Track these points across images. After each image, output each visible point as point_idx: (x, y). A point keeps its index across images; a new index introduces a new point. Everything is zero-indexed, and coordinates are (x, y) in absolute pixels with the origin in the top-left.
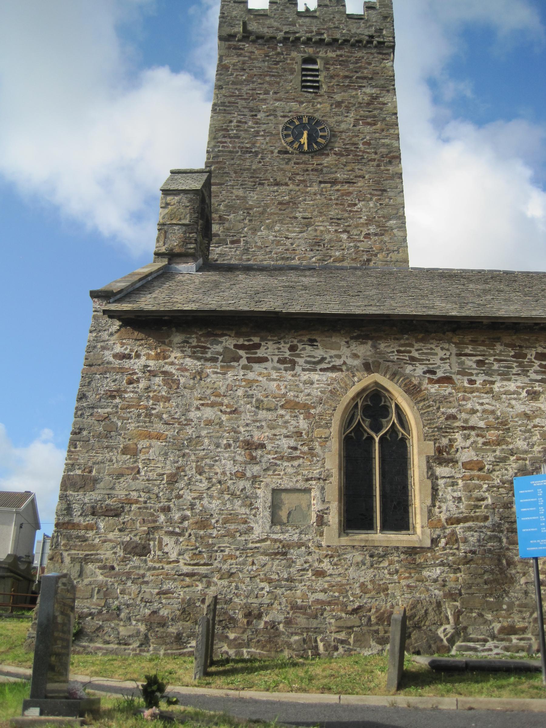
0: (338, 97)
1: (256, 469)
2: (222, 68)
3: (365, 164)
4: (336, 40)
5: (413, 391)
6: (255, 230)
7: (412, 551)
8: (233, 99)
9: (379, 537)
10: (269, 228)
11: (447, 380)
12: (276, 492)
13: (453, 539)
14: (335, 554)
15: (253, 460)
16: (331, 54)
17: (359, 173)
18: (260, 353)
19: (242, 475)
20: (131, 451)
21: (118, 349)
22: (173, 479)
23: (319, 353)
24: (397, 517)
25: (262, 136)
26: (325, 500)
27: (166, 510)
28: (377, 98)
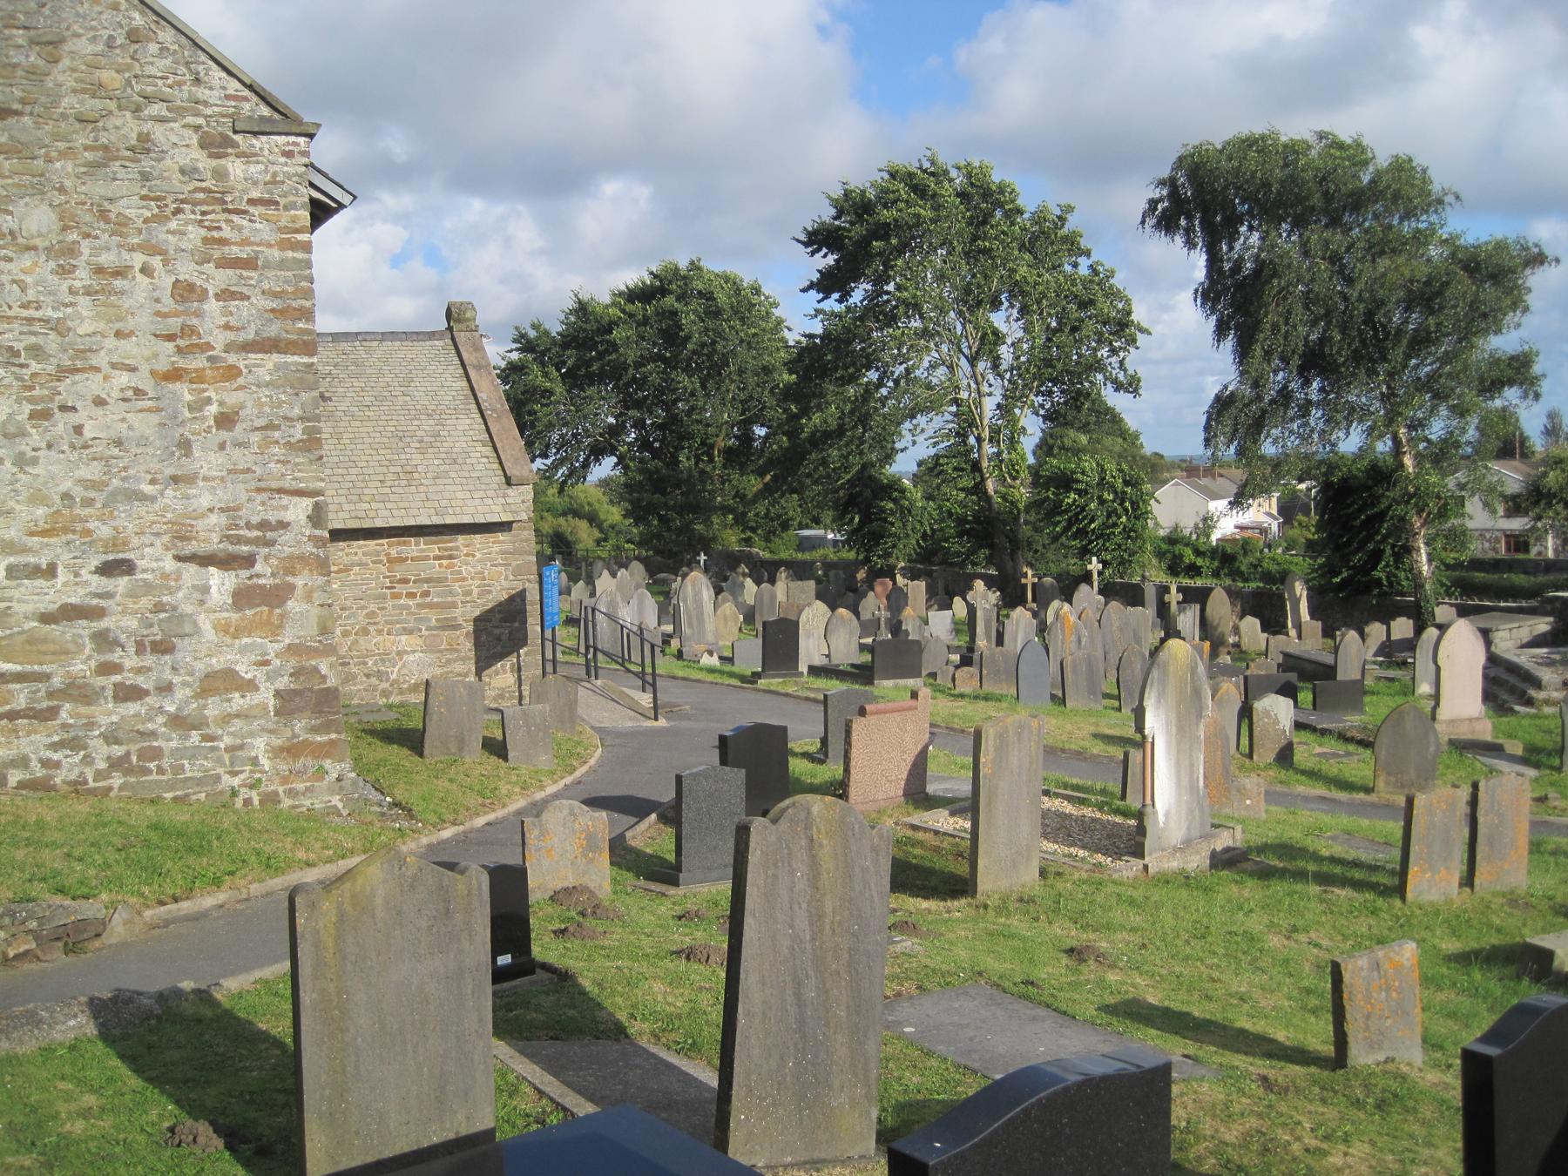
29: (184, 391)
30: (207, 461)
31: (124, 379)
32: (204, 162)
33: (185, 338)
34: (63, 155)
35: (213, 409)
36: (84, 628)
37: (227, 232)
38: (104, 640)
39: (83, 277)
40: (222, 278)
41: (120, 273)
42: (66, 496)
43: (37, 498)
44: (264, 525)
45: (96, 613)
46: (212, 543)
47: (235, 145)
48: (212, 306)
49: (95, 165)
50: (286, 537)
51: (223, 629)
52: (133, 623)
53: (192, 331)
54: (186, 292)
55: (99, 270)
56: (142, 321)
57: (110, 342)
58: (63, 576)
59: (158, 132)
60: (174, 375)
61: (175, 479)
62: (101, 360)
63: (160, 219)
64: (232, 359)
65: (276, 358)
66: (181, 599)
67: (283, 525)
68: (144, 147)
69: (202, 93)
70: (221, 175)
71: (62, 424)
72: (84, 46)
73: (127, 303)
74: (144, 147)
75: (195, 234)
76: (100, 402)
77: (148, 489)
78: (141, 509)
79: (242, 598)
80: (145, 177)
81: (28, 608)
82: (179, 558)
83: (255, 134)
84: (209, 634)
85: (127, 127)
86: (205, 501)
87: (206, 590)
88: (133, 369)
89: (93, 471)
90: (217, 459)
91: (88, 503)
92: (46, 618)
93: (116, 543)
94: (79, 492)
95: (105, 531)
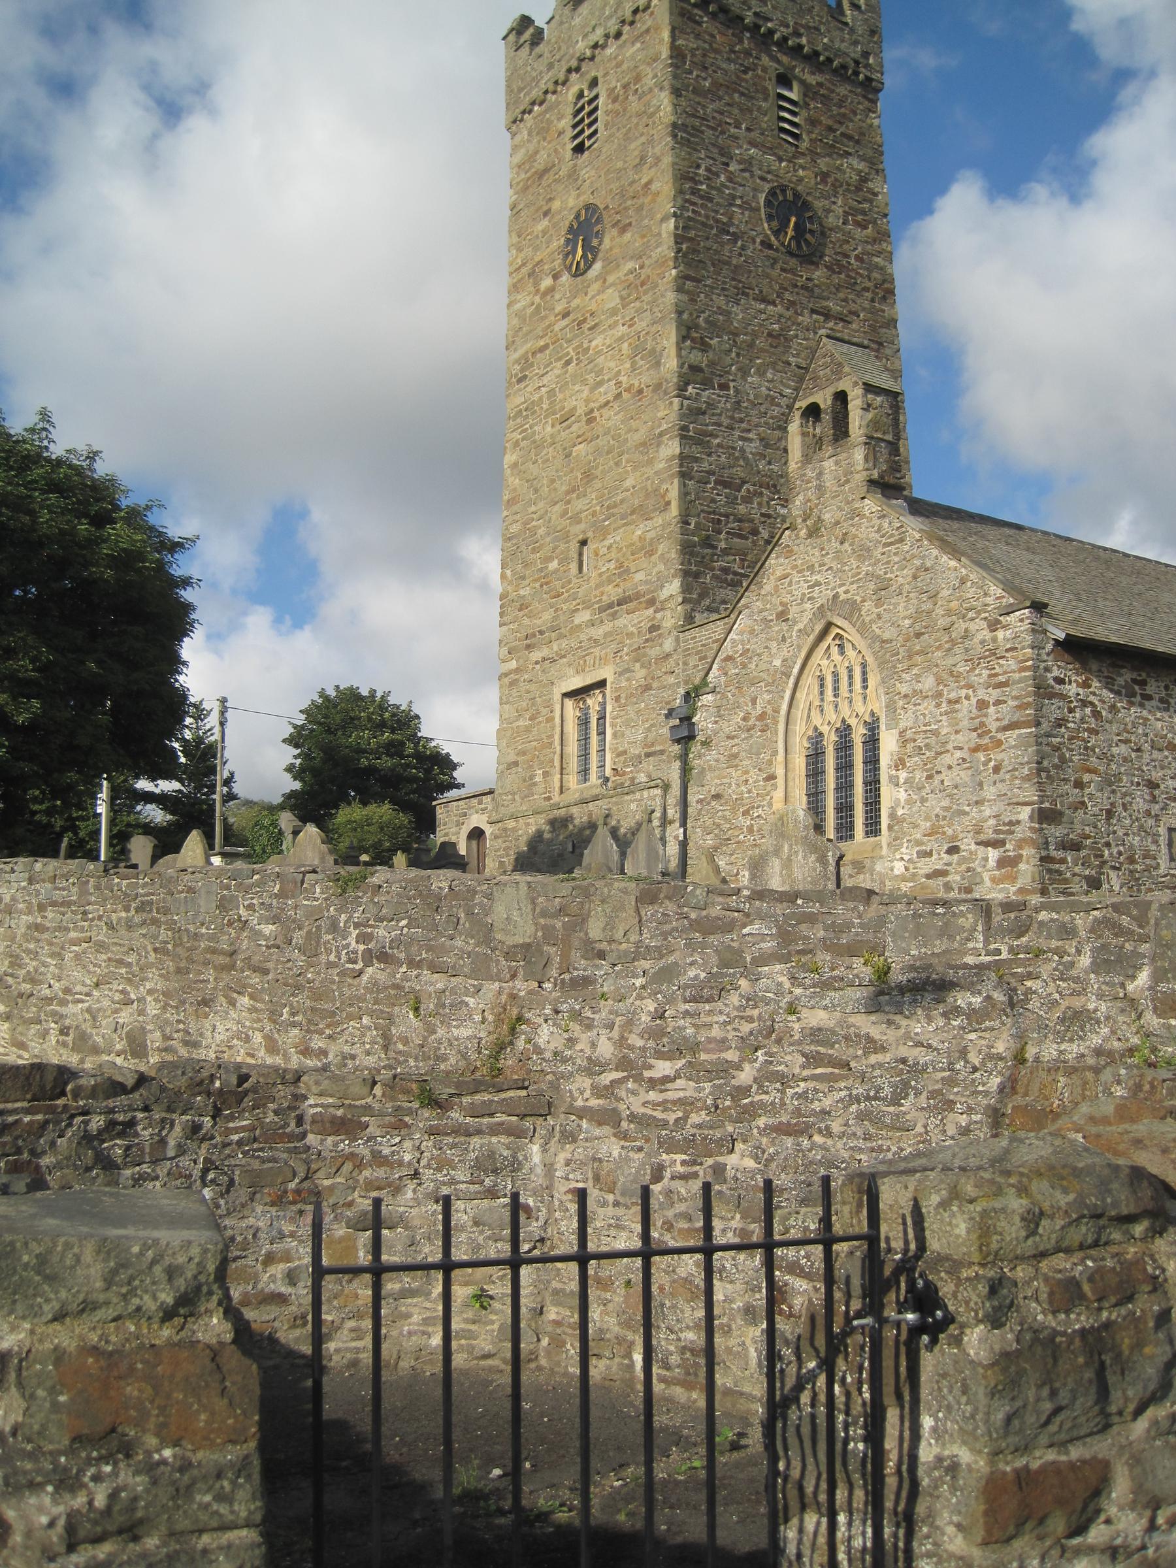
0: (823, 163)
1: (1156, 809)
2: (677, 54)
3: (859, 295)
4: (817, 54)
6: (745, 372)
10: (761, 373)
16: (812, 79)
18: (1149, 690)
20: (1079, 784)
22: (1110, 814)
25: (739, 206)
27: (1108, 845)
29: (981, 756)
30: (990, 792)
31: (958, 754)
32: (986, 634)
33: (980, 729)
34: (938, 648)
35: (992, 764)
36: (941, 881)
37: (998, 670)
39: (944, 707)
40: (995, 694)
41: (957, 701)
42: (937, 816)
43: (927, 819)
44: (1011, 823)
45: (941, 873)
46: (989, 835)
47: (999, 622)
48: (992, 709)
49: (949, 650)
50: (1018, 829)
51: (993, 880)
52: (958, 878)
53: (982, 724)
54: (982, 705)
55: (950, 702)
56: (965, 723)
57: (953, 737)
58: (935, 856)
59: (973, 627)
60: (976, 749)
61: (977, 803)
62: (950, 747)
63: (972, 670)
64: (999, 736)
65: (1017, 732)
66: (975, 865)
67: (1018, 822)
68: (967, 635)
69: (989, 600)
70: (995, 640)
71: (937, 778)
72: (945, 593)
73: (960, 715)
74: (967, 635)
75: (985, 673)
76: (950, 767)
77: (967, 809)
78: (965, 819)
79: (1002, 863)
80: (967, 650)
81: (922, 872)
82: (977, 844)
83: (1008, 614)
84: (988, 883)
85: (961, 625)
86: (988, 813)
87: (986, 859)
88: (961, 749)
89: (945, 803)
90: (993, 789)
91: (944, 818)
92: (928, 877)
93: (954, 838)
94: (941, 813)
95: (950, 832)
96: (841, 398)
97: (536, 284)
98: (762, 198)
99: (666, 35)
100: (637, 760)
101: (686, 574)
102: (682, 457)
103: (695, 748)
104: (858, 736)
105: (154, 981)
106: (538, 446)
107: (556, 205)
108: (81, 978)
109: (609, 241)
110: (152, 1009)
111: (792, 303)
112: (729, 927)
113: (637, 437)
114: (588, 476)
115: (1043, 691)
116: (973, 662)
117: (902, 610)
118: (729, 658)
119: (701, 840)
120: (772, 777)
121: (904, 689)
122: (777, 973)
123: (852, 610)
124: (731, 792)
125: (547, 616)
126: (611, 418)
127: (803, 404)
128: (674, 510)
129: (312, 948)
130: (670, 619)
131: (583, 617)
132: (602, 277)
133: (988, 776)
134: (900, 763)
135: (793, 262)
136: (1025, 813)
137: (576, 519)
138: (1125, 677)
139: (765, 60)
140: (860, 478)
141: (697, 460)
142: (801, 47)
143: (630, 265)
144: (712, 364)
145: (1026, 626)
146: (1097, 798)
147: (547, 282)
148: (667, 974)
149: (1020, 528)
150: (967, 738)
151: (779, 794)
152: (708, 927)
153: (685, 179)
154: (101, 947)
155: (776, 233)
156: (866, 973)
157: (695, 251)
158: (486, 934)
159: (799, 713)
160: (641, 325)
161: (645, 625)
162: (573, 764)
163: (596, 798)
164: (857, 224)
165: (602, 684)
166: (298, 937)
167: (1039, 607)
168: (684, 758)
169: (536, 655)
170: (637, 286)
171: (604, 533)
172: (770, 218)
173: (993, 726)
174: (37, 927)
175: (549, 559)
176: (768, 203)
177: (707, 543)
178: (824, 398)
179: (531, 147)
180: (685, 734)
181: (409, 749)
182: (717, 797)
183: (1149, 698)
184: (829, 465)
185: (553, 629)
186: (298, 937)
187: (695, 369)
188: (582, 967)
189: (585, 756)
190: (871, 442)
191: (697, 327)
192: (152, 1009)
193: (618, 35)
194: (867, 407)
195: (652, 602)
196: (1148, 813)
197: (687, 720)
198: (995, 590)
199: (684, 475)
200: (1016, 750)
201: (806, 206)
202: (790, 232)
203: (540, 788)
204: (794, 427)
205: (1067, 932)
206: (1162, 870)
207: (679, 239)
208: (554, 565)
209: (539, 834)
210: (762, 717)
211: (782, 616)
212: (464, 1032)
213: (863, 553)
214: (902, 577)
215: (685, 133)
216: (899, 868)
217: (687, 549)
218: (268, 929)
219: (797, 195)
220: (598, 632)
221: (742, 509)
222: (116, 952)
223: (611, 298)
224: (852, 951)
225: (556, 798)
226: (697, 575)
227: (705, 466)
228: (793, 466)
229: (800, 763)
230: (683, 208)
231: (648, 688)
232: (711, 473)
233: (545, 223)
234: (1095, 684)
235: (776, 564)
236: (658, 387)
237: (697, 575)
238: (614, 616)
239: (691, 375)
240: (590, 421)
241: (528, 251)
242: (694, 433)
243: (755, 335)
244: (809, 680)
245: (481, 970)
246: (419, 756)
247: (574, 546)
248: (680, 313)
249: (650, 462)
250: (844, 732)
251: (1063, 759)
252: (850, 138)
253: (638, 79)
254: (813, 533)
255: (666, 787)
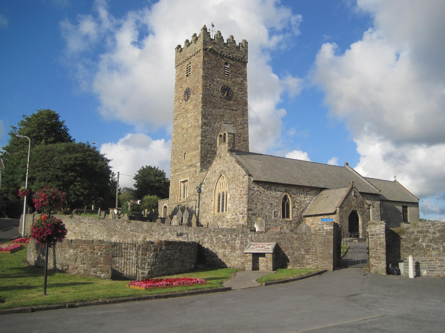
0: (233, 80)
2: (204, 62)
3: (240, 105)
4: (233, 58)
5: (291, 196)
6: (215, 123)
7: (290, 221)
8: (207, 75)
9: (286, 219)
10: (218, 123)
11: (294, 194)
12: (275, 212)
13: (295, 220)
14: (282, 222)
15: (272, 207)
16: (232, 63)
17: (238, 108)
19: (270, 209)
20: (256, 204)
21: (252, 186)
22: (262, 209)
23: (279, 188)
24: (288, 217)
26: (280, 214)
28: (242, 82)
30: (241, 205)
33: (241, 195)
38: (235, 221)
46: (241, 212)
54: (241, 191)
56: (239, 194)
60: (240, 198)
96: (225, 134)
97: (179, 101)
98: (220, 88)
99: (202, 58)
100: (192, 195)
101: (201, 162)
102: (201, 140)
103: (201, 194)
104: (225, 193)
105: (105, 233)
106: (178, 133)
107: (183, 86)
108: (96, 233)
109: (191, 96)
110: (105, 237)
111: (225, 108)
112: (165, 229)
113: (194, 135)
114: (186, 141)
115: (249, 189)
116: (240, 184)
117: (231, 173)
118: (207, 178)
119: (201, 210)
120: (212, 200)
121: (231, 187)
122: (169, 233)
123: (224, 172)
124: (206, 203)
125: (179, 166)
126: (190, 130)
127: (219, 134)
128: (200, 150)
129: (124, 230)
130: (198, 170)
131: (185, 168)
132: (190, 103)
133: (241, 203)
134: (230, 200)
135: (226, 100)
136: (246, 209)
137: (184, 149)
138: (267, 186)
139: (222, 60)
140: (227, 149)
141: (204, 140)
142: (230, 57)
143: (195, 102)
144: (208, 122)
145: (247, 178)
146: (259, 206)
147: (181, 101)
148: (159, 233)
149: (261, 155)
150: (239, 196)
151: (213, 203)
152: (163, 229)
153: (204, 86)
154: (98, 229)
155: (223, 95)
156: (176, 234)
157: (206, 100)
158: (143, 229)
159: (217, 189)
160: (196, 114)
161: (194, 171)
162: (182, 195)
163: (185, 202)
164: (240, 91)
165: (187, 180)
166: (123, 228)
167: (250, 175)
168: (199, 196)
169: (176, 174)
170: (195, 106)
171: (188, 152)
172: (221, 92)
173: (242, 194)
174: (90, 226)
175: (179, 156)
176: (221, 89)
177: (206, 156)
178: (222, 134)
179: (179, 73)
180: (200, 191)
181: (163, 181)
182: (204, 203)
183: (272, 189)
184: (223, 146)
185: (179, 169)
186: (123, 228)
187: (205, 123)
188: (152, 232)
189: (184, 194)
190: (229, 143)
191: (205, 115)
192: (105, 237)
193: (194, 55)
194: (229, 137)
195: (195, 166)
196: (270, 209)
197: (200, 189)
198: (244, 172)
199: (202, 143)
200: (245, 199)
201: (229, 89)
202: (226, 95)
203: (176, 199)
204: (218, 138)
205: (191, 230)
206: (273, 218)
207: (203, 98)
208: (180, 157)
209: (176, 208)
210: (211, 189)
211: (215, 172)
212: (140, 239)
213: (227, 163)
214: (232, 168)
215: (205, 77)
216: (229, 217)
217: (202, 157)
218: (120, 227)
219: (227, 87)
220: (187, 171)
221: (213, 149)
222: (100, 229)
223: (191, 107)
224: (175, 231)
225: (179, 201)
226: (203, 162)
227: (206, 141)
228: (217, 145)
229: (217, 198)
230: (204, 92)
231: (194, 182)
232: (207, 143)
233: (181, 89)
234: (261, 187)
235: (214, 163)
236: (198, 126)
237: (203, 162)
238: (189, 168)
239: (204, 124)
240: (187, 130)
241: (178, 94)
242: (204, 135)
243: (217, 115)
244: (218, 184)
245: (142, 233)
246: (165, 183)
247: (183, 154)
248: (202, 113)
249: (196, 140)
250: (223, 193)
251: (253, 200)
252: (240, 74)
253: (197, 65)
254: (220, 158)
255: (196, 201)
